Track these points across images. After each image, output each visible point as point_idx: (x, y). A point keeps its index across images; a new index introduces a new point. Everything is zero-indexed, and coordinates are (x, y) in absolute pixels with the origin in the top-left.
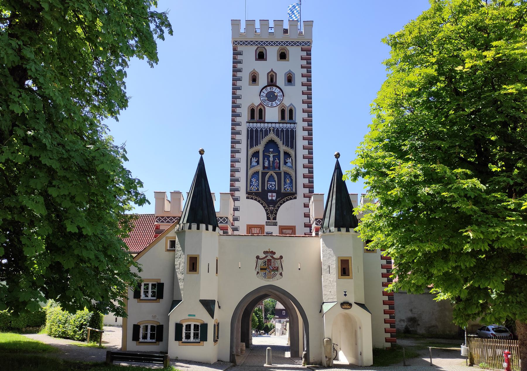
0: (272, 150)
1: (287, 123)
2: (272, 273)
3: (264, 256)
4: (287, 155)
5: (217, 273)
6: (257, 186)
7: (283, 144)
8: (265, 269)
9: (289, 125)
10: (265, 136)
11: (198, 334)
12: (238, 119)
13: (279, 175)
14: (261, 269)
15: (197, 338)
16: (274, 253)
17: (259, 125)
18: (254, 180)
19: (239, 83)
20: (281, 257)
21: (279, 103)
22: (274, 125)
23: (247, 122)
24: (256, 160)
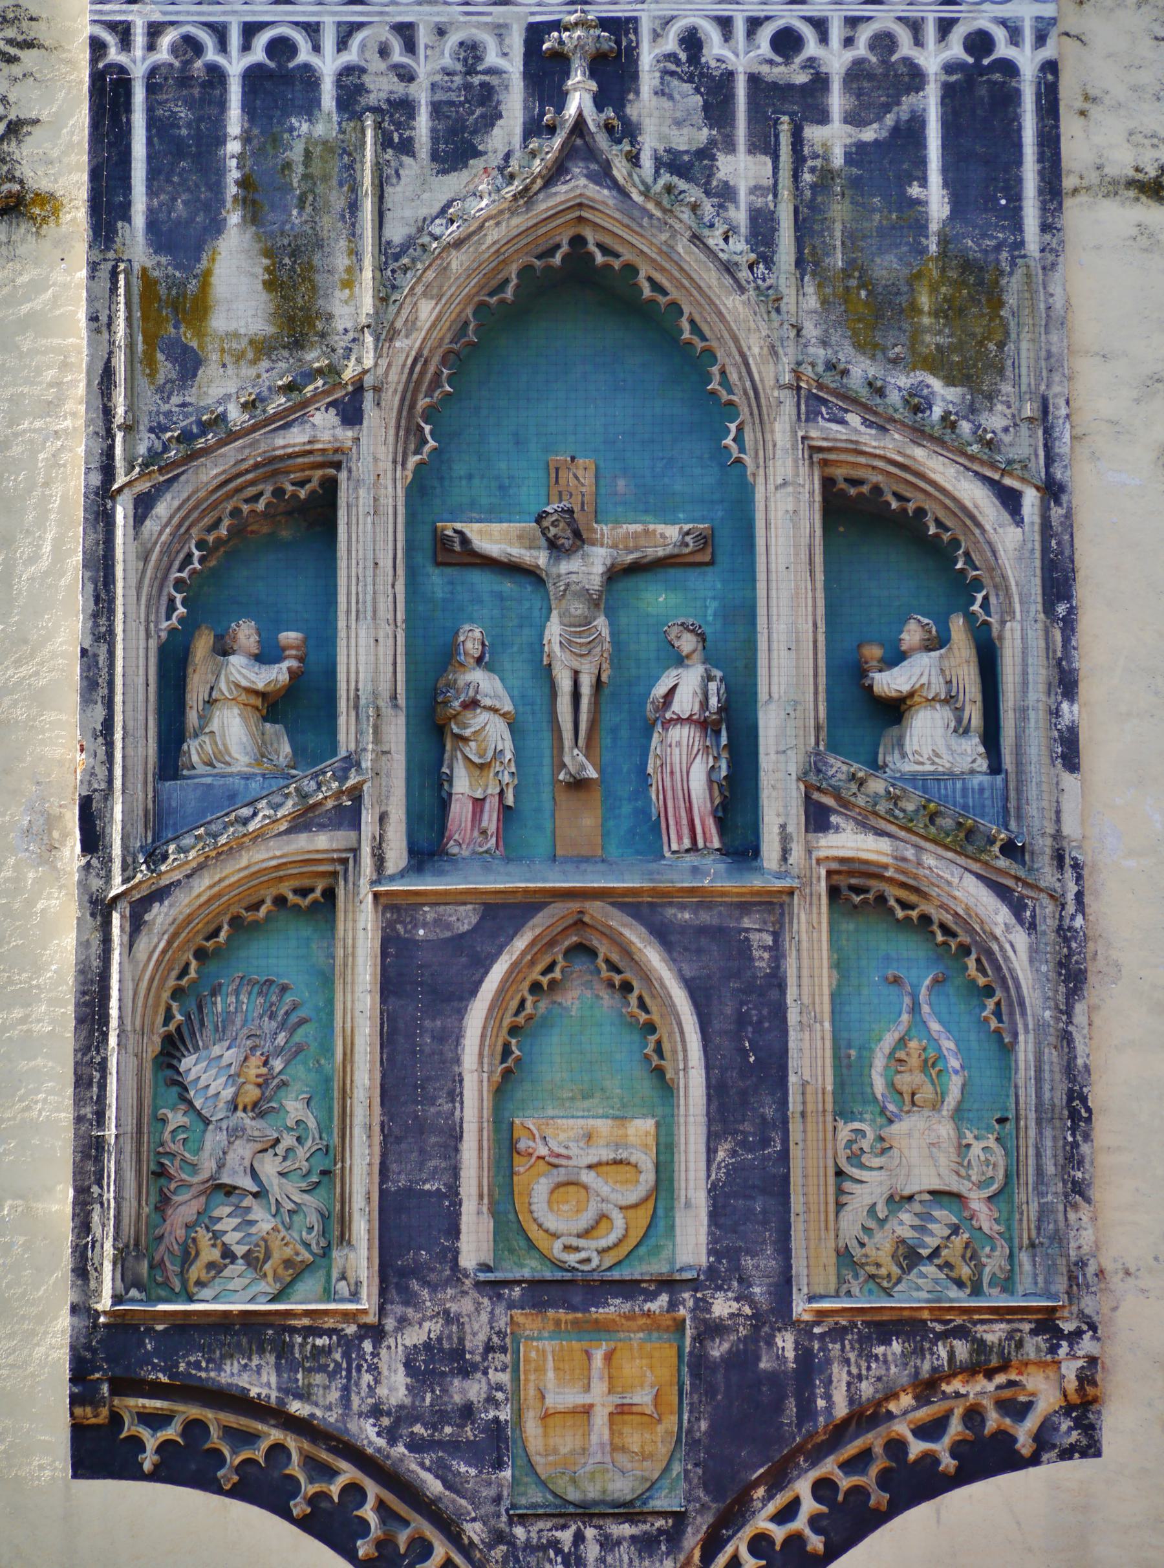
24: (276, 675)
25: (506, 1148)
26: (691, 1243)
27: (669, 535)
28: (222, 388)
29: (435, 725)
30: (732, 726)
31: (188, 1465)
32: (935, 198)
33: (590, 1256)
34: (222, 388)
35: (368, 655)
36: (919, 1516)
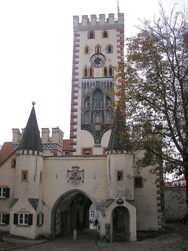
1: (108, 78)
2: (77, 181)
8: (73, 179)
12: (76, 77)
14: (70, 179)
15: (27, 223)
16: (79, 168)
17: (89, 79)
19: (77, 54)
20: (83, 171)
22: (99, 79)
25: (95, 119)
26: (101, 122)
27: (101, 98)
28: (86, 94)
29: (93, 105)
30: (103, 104)
32: (110, 86)
33: (98, 122)
34: (86, 94)
35: (91, 102)
36: (108, 131)
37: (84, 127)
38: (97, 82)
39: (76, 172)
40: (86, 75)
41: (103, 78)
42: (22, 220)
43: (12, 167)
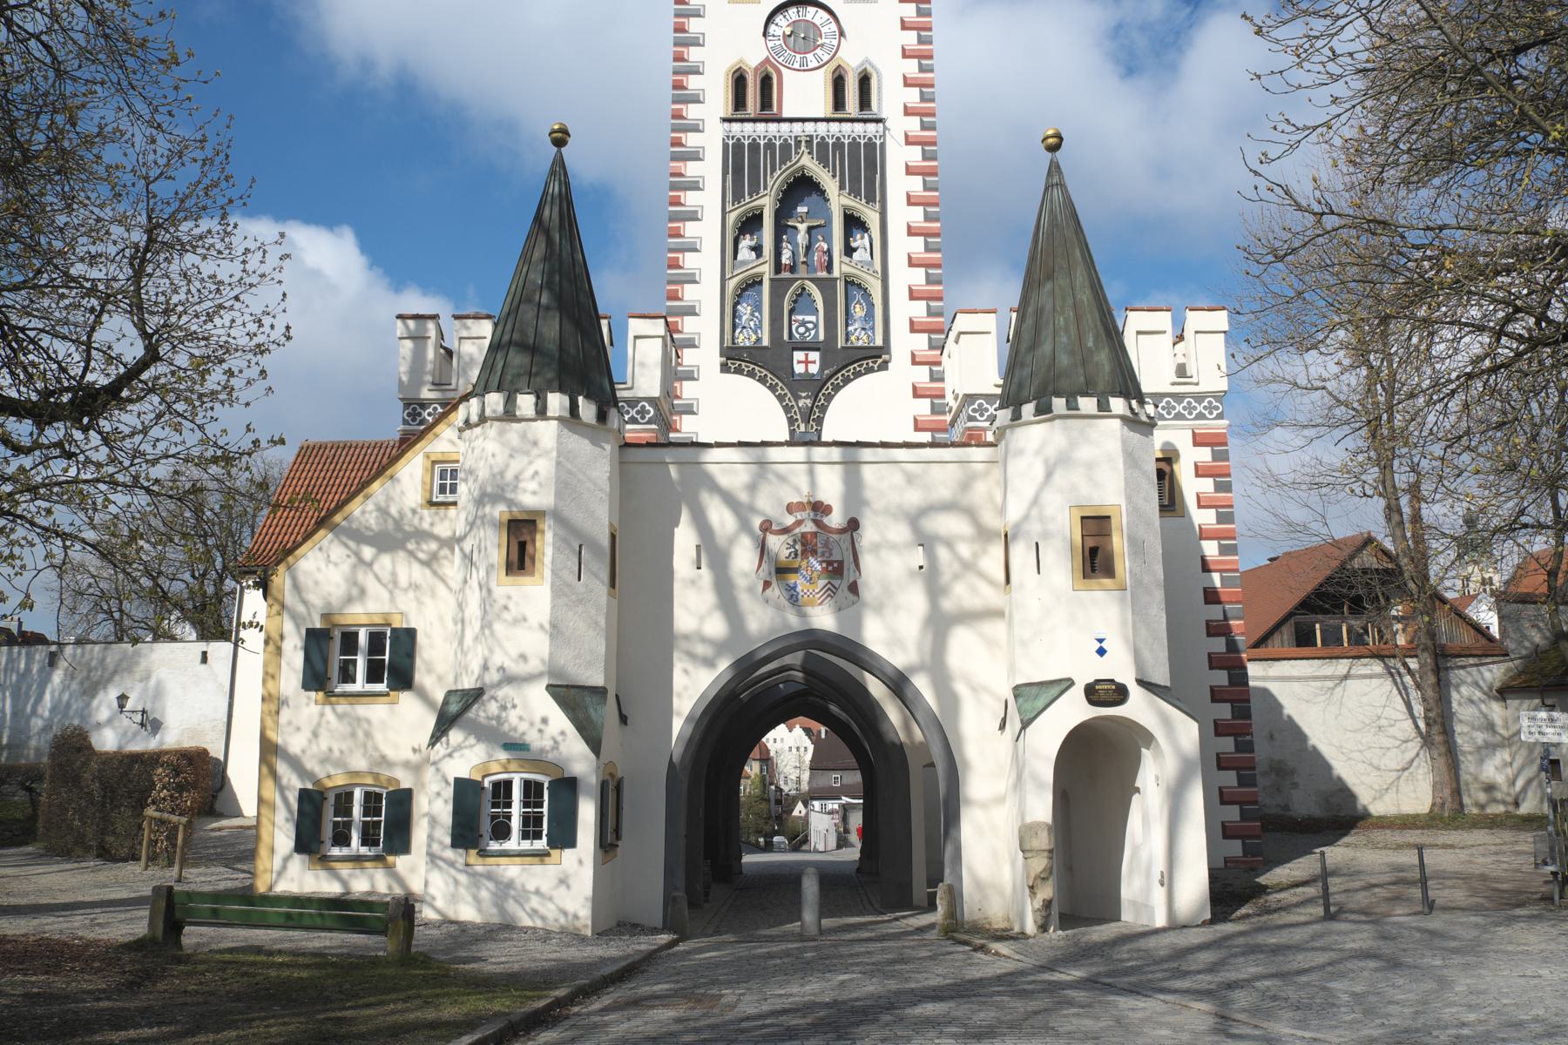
0: (805, 209)
1: (852, 120)
3: (789, 520)
4: (853, 223)
5: (613, 584)
6: (756, 331)
7: (842, 187)
9: (859, 127)
10: (783, 162)
11: (538, 820)
13: (827, 286)
15: (538, 836)
16: (827, 510)
17: (761, 127)
18: (745, 309)
21: (826, 58)
22: (810, 128)
23: (725, 120)
24: (753, 243)
26: (822, 337)
31: (739, 371)
37: (735, 358)
38: (798, 143)
39: (815, 534)
40: (739, 101)
41: (828, 120)
42: (509, 817)
43: (431, 504)
